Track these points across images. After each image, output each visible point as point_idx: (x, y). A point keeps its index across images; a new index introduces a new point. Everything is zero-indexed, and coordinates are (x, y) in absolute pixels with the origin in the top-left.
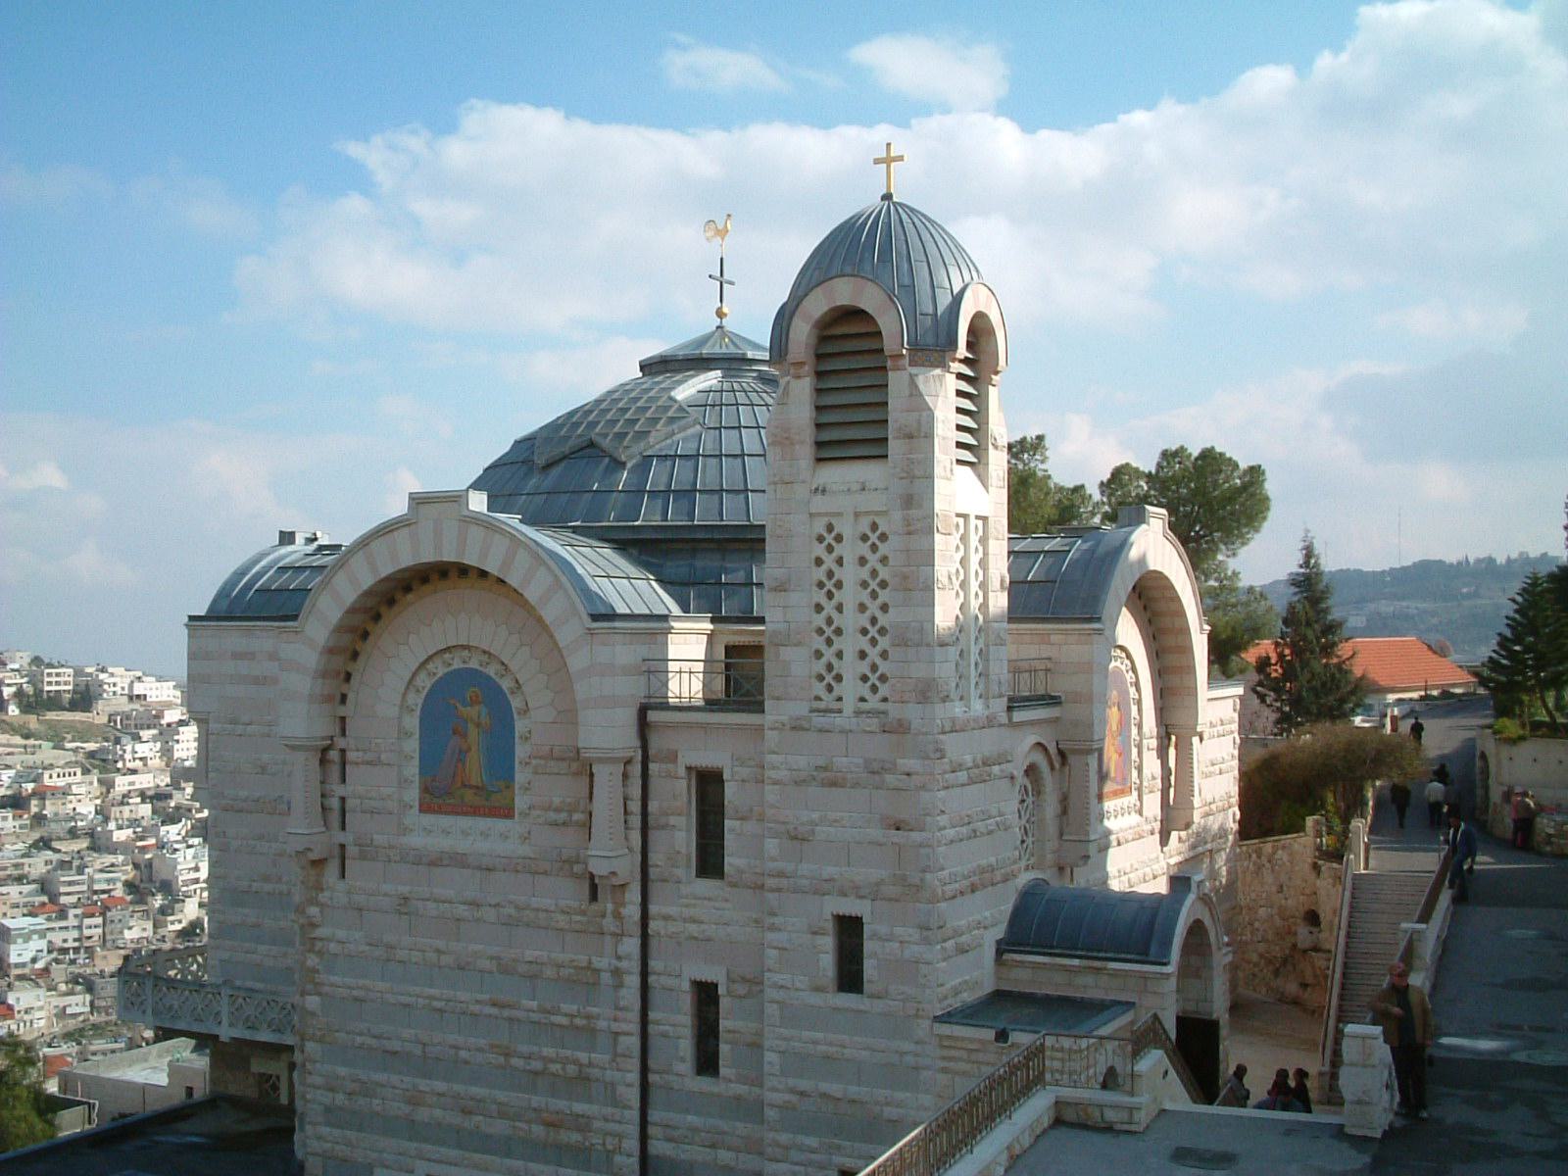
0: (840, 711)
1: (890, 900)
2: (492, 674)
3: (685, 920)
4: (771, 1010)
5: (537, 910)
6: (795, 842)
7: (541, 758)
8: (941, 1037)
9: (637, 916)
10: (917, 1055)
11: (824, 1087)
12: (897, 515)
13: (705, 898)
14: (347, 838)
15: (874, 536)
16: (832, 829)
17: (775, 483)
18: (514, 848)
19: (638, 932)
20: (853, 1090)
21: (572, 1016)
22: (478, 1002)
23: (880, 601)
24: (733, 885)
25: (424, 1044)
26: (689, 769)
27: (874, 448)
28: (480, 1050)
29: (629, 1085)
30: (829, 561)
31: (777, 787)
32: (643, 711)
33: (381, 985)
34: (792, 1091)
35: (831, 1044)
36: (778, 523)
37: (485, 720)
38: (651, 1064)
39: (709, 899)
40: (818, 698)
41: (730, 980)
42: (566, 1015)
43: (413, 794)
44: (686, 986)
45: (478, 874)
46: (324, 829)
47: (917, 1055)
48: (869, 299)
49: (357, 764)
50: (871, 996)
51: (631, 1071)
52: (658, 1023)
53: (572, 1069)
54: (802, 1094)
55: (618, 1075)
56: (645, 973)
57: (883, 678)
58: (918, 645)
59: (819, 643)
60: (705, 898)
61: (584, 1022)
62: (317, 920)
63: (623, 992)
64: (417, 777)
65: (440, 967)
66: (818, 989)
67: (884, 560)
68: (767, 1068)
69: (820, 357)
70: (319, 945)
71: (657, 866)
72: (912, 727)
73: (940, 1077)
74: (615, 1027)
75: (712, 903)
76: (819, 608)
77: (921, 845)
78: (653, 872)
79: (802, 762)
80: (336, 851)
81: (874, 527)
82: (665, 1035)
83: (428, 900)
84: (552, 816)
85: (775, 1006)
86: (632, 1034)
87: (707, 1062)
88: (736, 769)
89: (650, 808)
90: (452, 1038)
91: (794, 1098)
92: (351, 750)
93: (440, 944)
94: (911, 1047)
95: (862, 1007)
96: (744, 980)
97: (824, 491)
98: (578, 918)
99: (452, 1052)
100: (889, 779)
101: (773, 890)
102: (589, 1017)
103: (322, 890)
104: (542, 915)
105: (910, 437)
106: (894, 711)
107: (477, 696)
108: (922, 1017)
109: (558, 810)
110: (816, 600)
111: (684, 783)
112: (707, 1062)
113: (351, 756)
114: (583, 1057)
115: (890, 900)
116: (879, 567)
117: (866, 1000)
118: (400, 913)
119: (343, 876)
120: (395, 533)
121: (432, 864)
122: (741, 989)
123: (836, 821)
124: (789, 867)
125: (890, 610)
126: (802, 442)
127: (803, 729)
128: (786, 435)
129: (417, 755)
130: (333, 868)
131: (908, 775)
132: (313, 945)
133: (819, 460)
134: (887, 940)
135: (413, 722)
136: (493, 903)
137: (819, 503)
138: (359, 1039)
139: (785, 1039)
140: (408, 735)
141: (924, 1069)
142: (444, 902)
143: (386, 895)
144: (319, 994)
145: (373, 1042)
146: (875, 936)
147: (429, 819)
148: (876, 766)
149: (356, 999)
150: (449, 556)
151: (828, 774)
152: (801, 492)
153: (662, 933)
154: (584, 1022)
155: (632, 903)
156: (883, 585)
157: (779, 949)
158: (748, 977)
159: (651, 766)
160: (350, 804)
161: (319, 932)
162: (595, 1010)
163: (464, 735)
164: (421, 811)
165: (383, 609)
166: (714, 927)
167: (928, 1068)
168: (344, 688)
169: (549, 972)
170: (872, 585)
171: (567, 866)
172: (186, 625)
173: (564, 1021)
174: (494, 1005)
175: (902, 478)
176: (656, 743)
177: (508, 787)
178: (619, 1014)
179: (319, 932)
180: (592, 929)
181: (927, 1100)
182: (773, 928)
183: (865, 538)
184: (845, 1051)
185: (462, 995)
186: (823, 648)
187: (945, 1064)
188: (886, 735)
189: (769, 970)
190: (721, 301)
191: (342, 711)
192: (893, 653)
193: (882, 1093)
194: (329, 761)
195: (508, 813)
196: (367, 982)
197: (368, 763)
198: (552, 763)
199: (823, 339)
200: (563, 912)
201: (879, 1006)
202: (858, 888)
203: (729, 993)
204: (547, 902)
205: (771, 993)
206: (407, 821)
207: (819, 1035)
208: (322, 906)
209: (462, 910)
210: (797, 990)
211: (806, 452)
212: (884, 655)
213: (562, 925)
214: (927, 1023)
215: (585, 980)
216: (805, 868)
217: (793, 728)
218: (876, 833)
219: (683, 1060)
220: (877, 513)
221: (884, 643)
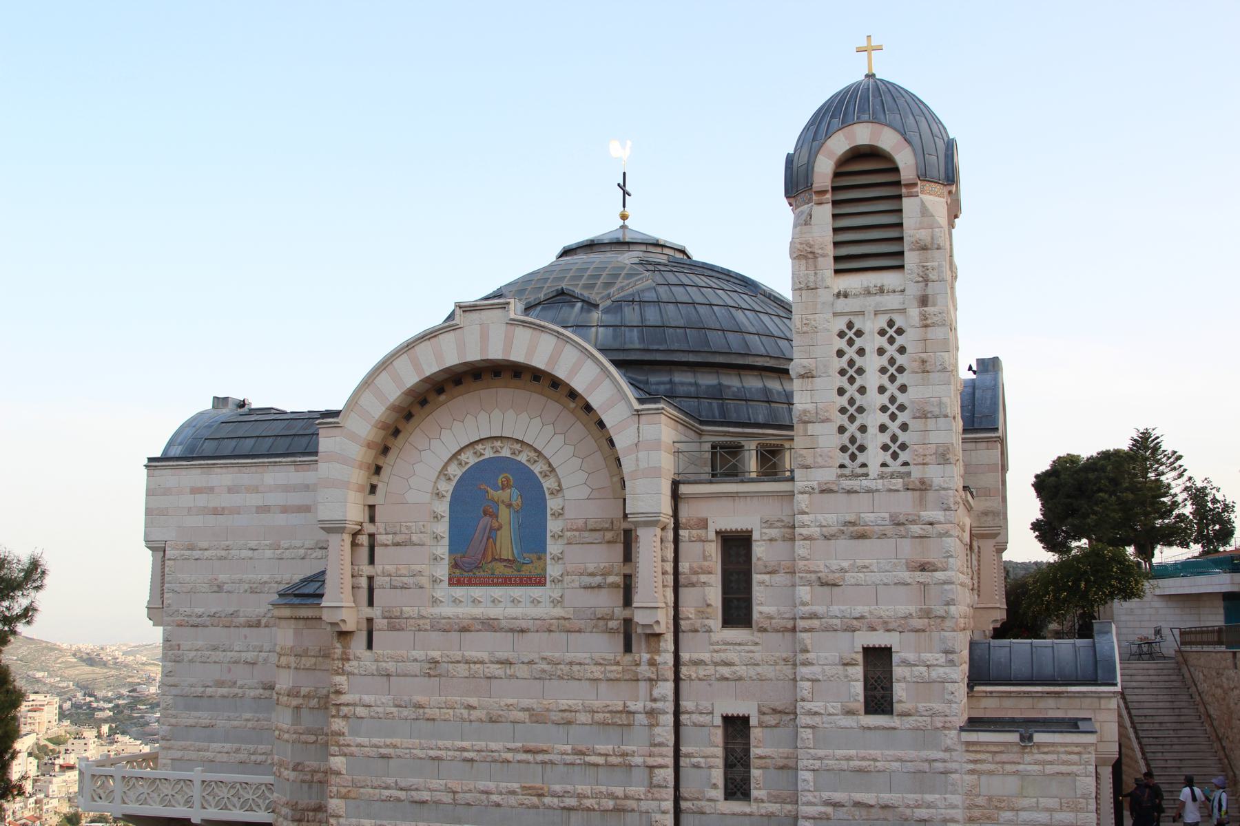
0: (866, 475)
1: (917, 631)
2: (524, 460)
3: (716, 664)
4: (806, 734)
5: (571, 664)
6: (825, 588)
7: (576, 530)
8: (968, 743)
9: (671, 662)
10: (945, 761)
11: (859, 797)
12: (914, 312)
13: (735, 644)
14: (375, 613)
15: (890, 331)
16: (860, 575)
17: (800, 289)
18: (545, 611)
19: (671, 675)
20: (886, 798)
21: (607, 755)
22: (510, 750)
23: (898, 383)
24: (763, 630)
25: (454, 792)
26: (717, 533)
28: (513, 793)
29: (664, 812)
30: (851, 353)
31: (808, 542)
32: (675, 485)
33: (408, 742)
34: (827, 803)
35: (864, 759)
36: (805, 322)
37: (517, 502)
38: (684, 791)
39: (740, 644)
40: (842, 466)
41: (762, 713)
42: (600, 755)
43: (443, 571)
44: (718, 721)
45: (510, 634)
46: (353, 605)
47: (945, 761)
48: (887, 140)
49: (386, 545)
50: (901, 715)
51: (666, 800)
52: (689, 756)
53: (610, 804)
54: (836, 805)
55: (654, 804)
56: (677, 713)
57: (903, 447)
58: (936, 417)
59: (843, 420)
60: (735, 644)
61: (620, 760)
62: (345, 687)
63: (657, 730)
64: (447, 554)
65: (471, 721)
66: (850, 713)
67: (902, 350)
68: (801, 785)
70: (345, 710)
71: (688, 618)
72: (934, 485)
73: (966, 777)
74: (651, 761)
75: (742, 647)
76: (841, 392)
77: (945, 583)
78: (684, 624)
79: (831, 519)
80: (364, 625)
81: (891, 323)
82: (696, 766)
83: (458, 662)
84: (587, 580)
85: (809, 731)
86: (666, 767)
87: (737, 788)
88: (764, 530)
89: (680, 569)
90: (482, 785)
91: (829, 810)
92: (380, 534)
93: (473, 701)
94: (941, 755)
95: (893, 725)
96: (775, 711)
97: (846, 296)
98: (614, 668)
99: (484, 797)
100: (916, 529)
101: (806, 630)
102: (624, 755)
103: (348, 660)
104: (576, 668)
105: (924, 248)
106: (916, 473)
107: (508, 480)
108: (949, 729)
109: (592, 575)
111: (713, 545)
112: (737, 788)
113: (380, 538)
114: (619, 791)
115: (917, 631)
116: (897, 356)
117: (895, 718)
118: (430, 676)
119: (370, 646)
120: (440, 336)
121: (464, 630)
122: (770, 719)
123: (866, 567)
124: (820, 609)
125: (910, 389)
126: (823, 256)
127: (831, 491)
128: (809, 250)
129: (447, 535)
130: (362, 638)
131: (931, 524)
132: (338, 711)
133: (837, 272)
134: (915, 665)
135: (443, 508)
136: (526, 661)
137: (842, 304)
138: (386, 793)
139: (820, 759)
140: (437, 518)
141: (951, 773)
142: (475, 663)
143: (416, 660)
144: (345, 755)
145: (402, 795)
146: (906, 663)
147: (459, 592)
148: (902, 519)
149: (383, 757)
150: (496, 353)
151: (856, 528)
152: (825, 296)
153: (694, 676)
154: (620, 760)
155: (667, 651)
156: (901, 370)
157: (813, 681)
158: (779, 709)
159: (681, 532)
160: (378, 581)
161: (344, 699)
162: (629, 748)
163: (495, 516)
164: (451, 584)
165: (416, 410)
166: (744, 667)
167: (955, 772)
168: (374, 480)
169: (583, 718)
170: (892, 371)
171: (601, 623)
172: (146, 466)
173: (601, 760)
174: (527, 751)
175: (918, 282)
176: (685, 512)
177: (539, 558)
178: (656, 750)
179: (344, 699)
180: (627, 677)
181: (956, 799)
182: (804, 664)
183: (882, 333)
184: (878, 764)
185: (493, 745)
186: (846, 423)
187: (972, 766)
188: (909, 493)
189: (803, 700)
190: (624, 206)
191: (372, 500)
192: (913, 424)
193: (911, 798)
194: (357, 545)
195: (540, 581)
196: (394, 741)
197: (397, 544)
198: (586, 534)
199: (837, 175)
200: (597, 664)
201: (910, 722)
202: (886, 623)
203: (761, 725)
204: (580, 656)
205: (803, 720)
206: (439, 594)
207: (853, 752)
208: (349, 674)
209: (495, 670)
210: (829, 714)
211: (828, 265)
212: (904, 427)
213: (598, 675)
214: (954, 733)
215: (622, 720)
216: (835, 609)
217: (822, 491)
218: (906, 575)
219: (715, 786)
220: (892, 311)
221: (902, 417)
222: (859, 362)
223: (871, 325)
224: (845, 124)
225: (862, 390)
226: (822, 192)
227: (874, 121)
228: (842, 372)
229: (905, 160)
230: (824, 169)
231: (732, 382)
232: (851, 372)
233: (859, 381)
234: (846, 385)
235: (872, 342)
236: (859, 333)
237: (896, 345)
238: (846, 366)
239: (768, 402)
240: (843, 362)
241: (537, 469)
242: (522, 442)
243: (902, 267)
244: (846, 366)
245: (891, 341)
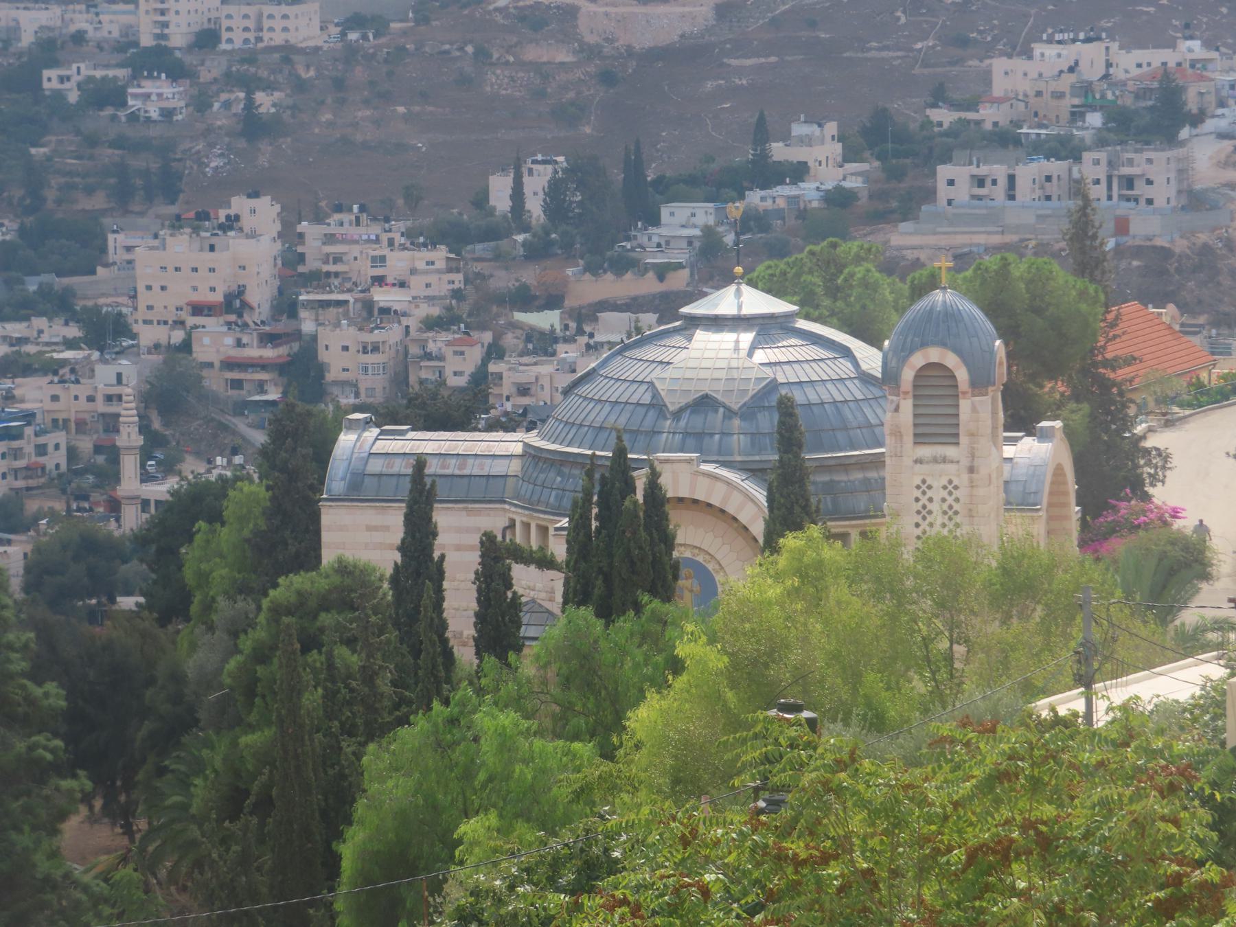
2: (701, 561)
12: (965, 477)
27: (953, 439)
30: (924, 500)
37: (696, 588)
48: (951, 360)
67: (957, 500)
69: (915, 387)
76: (917, 525)
105: (972, 435)
110: (916, 521)
116: (954, 504)
152: (908, 461)
156: (956, 513)
183: (945, 488)
211: (909, 439)
222: (930, 506)
223: (937, 483)
224: (924, 345)
225: (931, 525)
226: (906, 393)
227: (943, 344)
228: (918, 512)
229: (962, 375)
230: (908, 375)
231: (841, 477)
232: (924, 512)
233: (929, 519)
234: (920, 521)
235: (940, 494)
236: (930, 487)
237: (953, 497)
238: (920, 509)
239: (868, 491)
240: (919, 506)
241: (710, 567)
242: (700, 549)
243: (957, 444)
244: (920, 509)
245: (950, 493)
